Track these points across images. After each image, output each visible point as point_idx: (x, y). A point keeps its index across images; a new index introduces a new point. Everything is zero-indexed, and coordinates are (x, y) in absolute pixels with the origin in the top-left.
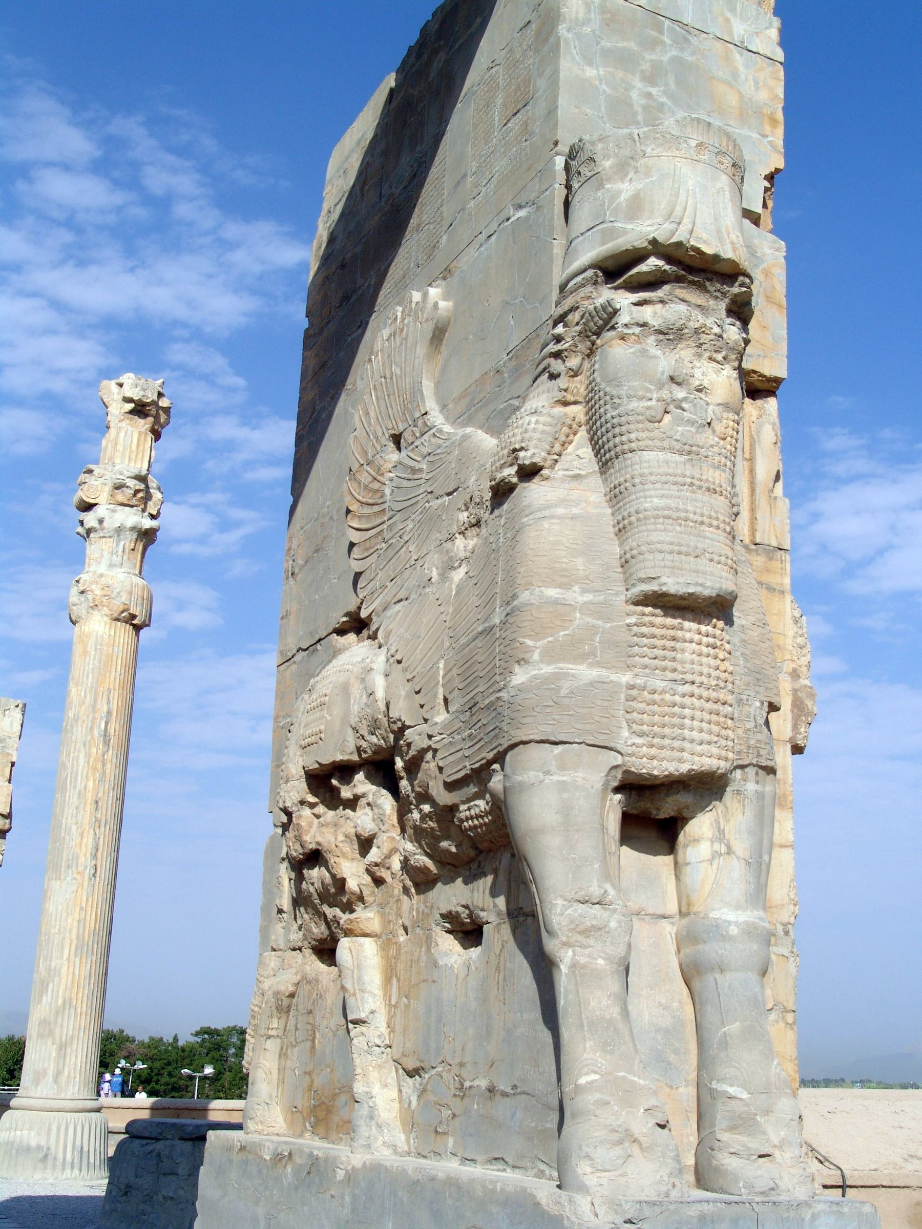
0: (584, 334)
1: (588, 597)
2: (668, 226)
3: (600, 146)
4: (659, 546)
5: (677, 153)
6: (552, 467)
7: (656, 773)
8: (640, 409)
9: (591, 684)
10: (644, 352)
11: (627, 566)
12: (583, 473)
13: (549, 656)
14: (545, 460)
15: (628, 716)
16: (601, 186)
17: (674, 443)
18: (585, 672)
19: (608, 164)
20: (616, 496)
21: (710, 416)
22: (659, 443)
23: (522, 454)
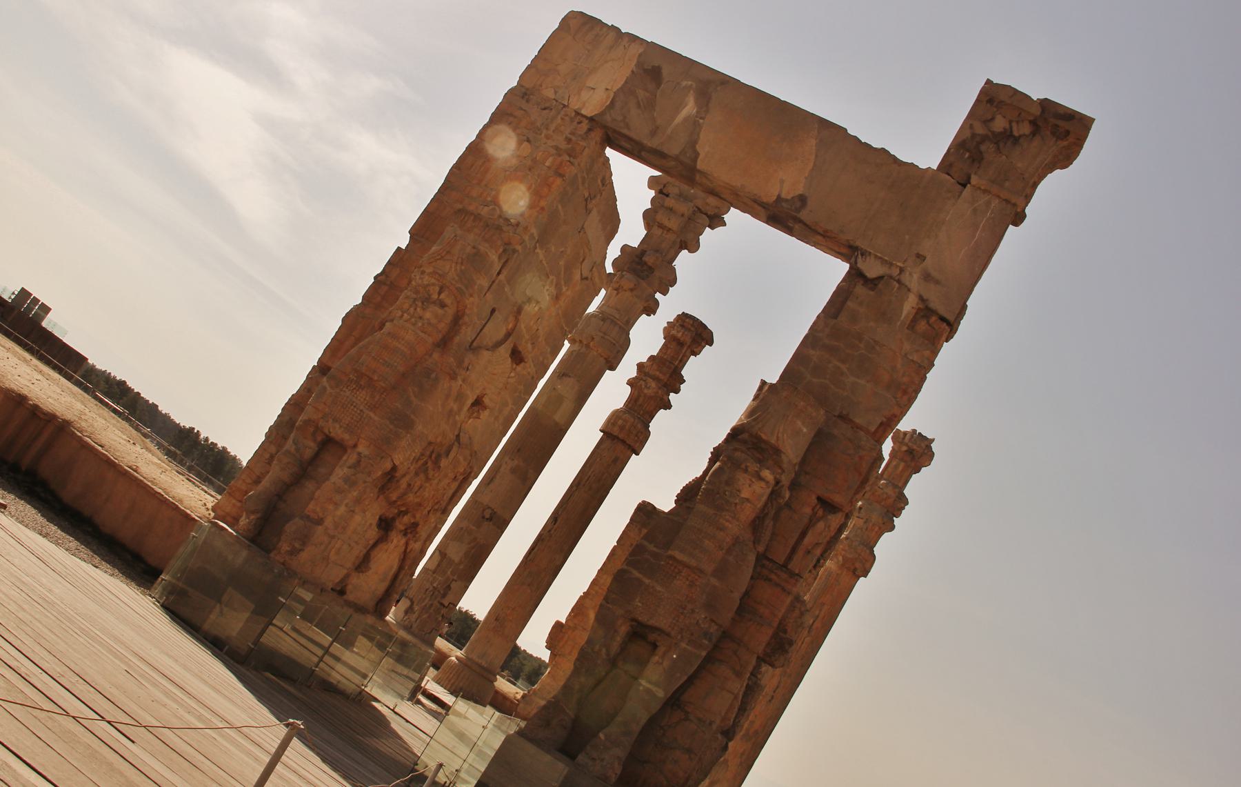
1: (655, 549)
7: (640, 619)
21: (737, 501)
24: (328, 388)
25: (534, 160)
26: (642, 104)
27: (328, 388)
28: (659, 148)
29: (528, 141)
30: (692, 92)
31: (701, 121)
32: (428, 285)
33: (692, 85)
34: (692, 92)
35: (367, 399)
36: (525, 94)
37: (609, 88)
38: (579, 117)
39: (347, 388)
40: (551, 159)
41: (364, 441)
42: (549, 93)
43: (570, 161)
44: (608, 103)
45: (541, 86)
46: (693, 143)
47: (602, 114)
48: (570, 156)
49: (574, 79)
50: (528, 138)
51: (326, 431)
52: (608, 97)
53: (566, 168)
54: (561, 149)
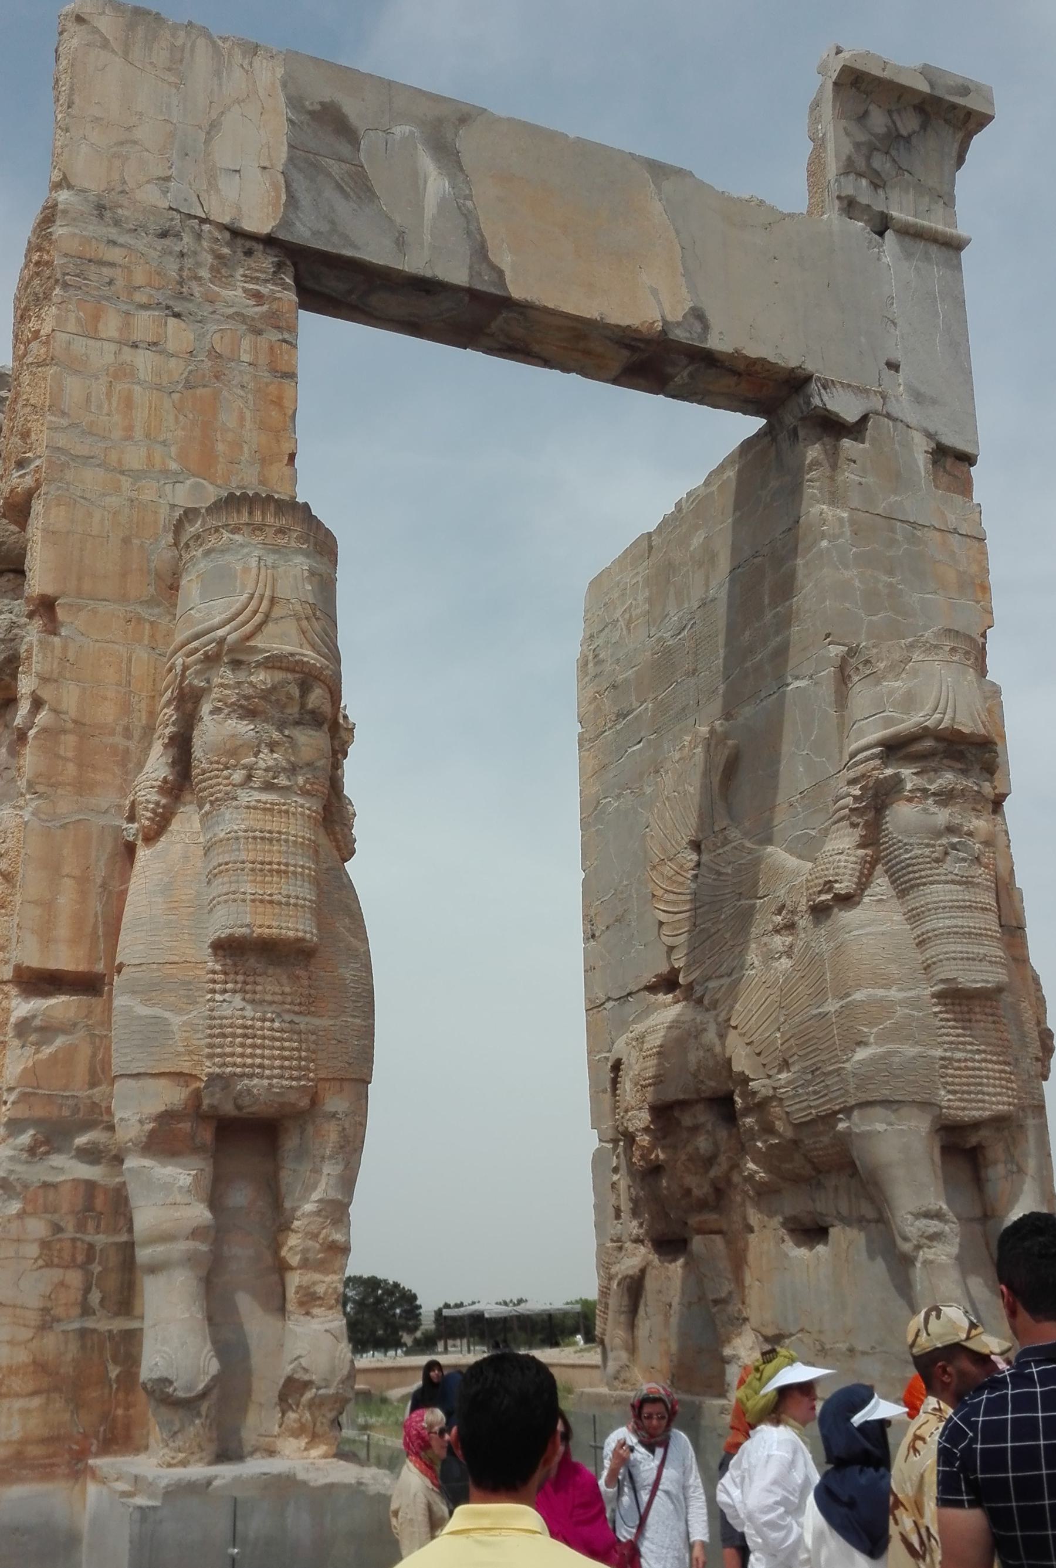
0: (876, 796)
2: (937, 716)
3: (875, 651)
4: (953, 955)
5: (936, 658)
6: (861, 895)
8: (927, 853)
9: (914, 1058)
10: (925, 810)
11: (928, 970)
12: (884, 897)
13: (881, 1039)
14: (855, 890)
15: (942, 1080)
16: (878, 682)
17: (954, 877)
18: (911, 1051)
19: (882, 665)
20: (914, 917)
22: (943, 878)
23: (837, 885)
24: (167, 1015)
25: (214, 355)
26: (348, 190)
27: (167, 1015)
28: (428, 274)
29: (177, 315)
30: (420, 147)
31: (469, 203)
32: (274, 688)
33: (412, 133)
34: (420, 147)
35: (287, 989)
36: (101, 209)
37: (267, 164)
38: (240, 242)
39: (225, 991)
40: (246, 344)
41: (327, 1086)
42: (151, 196)
43: (285, 341)
44: (284, 197)
45: (124, 182)
46: (481, 252)
47: (285, 223)
48: (278, 328)
49: (187, 155)
50: (168, 307)
51: (229, 1109)
52: (276, 189)
53: (286, 357)
54: (253, 319)
